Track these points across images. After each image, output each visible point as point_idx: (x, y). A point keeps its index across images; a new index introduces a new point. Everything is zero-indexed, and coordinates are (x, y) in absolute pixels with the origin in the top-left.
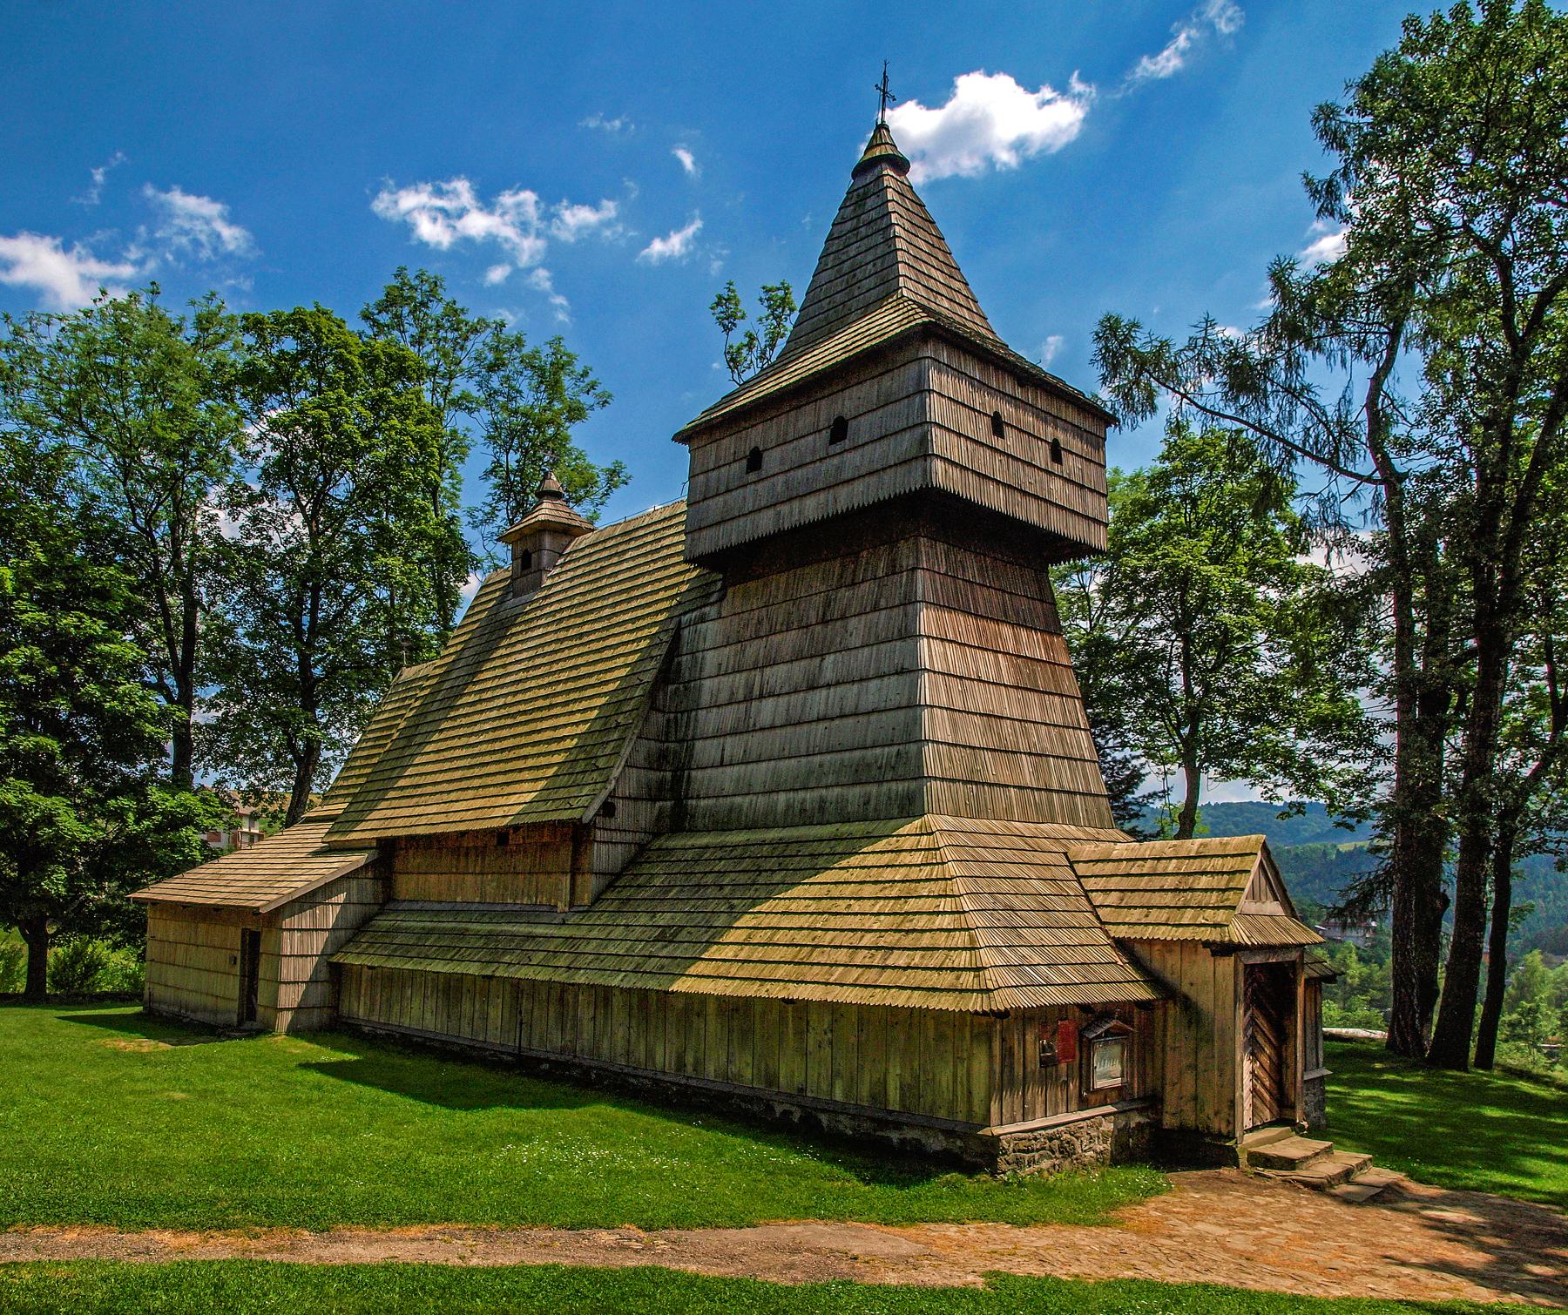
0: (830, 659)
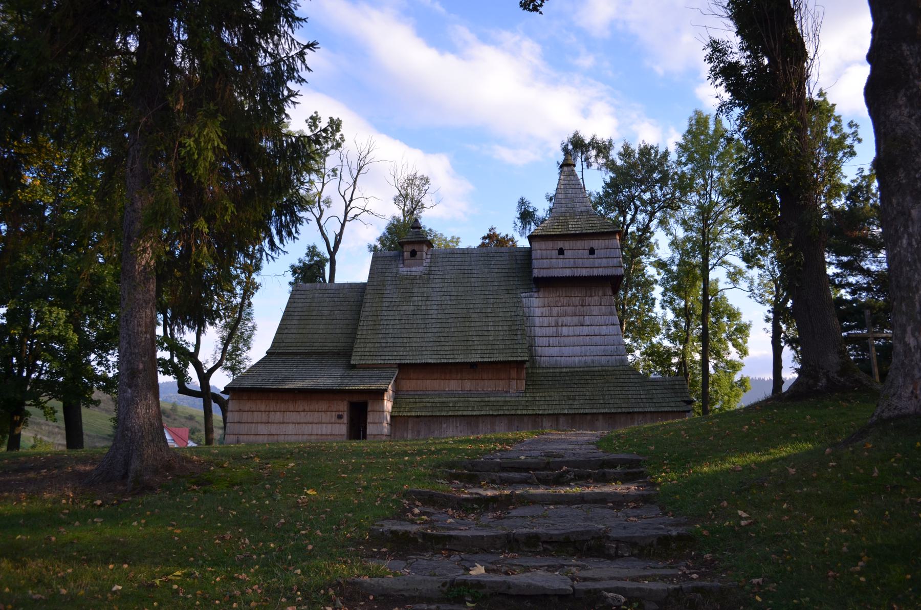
0: (587, 318)
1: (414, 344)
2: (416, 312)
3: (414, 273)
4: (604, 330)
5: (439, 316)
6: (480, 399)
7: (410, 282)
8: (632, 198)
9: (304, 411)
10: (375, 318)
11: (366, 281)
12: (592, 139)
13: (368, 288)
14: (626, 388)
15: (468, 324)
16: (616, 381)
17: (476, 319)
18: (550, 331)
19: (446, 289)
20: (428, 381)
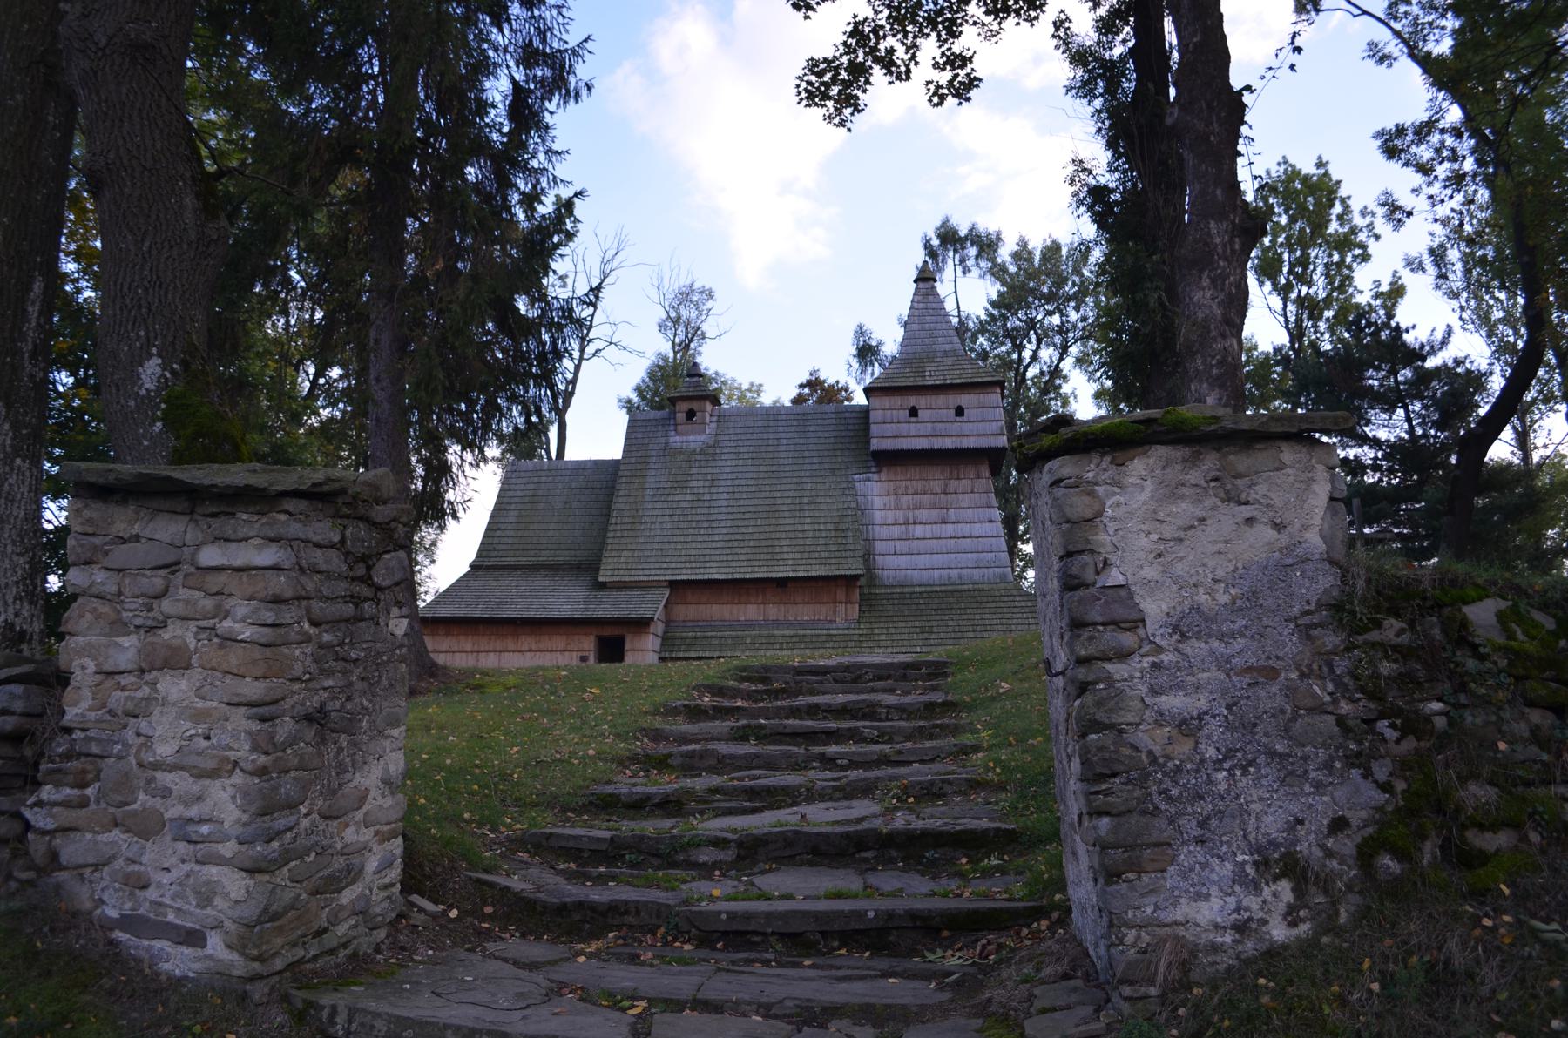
1: (693, 552)
2: (695, 504)
3: (692, 445)
4: (977, 529)
5: (730, 510)
6: (792, 633)
7: (686, 458)
8: (1031, 324)
9: (530, 651)
10: (633, 513)
11: (618, 455)
12: (972, 230)
13: (622, 467)
14: (1008, 616)
15: (774, 521)
16: (994, 605)
17: (786, 514)
18: (896, 531)
19: (740, 469)
20: (714, 607)
